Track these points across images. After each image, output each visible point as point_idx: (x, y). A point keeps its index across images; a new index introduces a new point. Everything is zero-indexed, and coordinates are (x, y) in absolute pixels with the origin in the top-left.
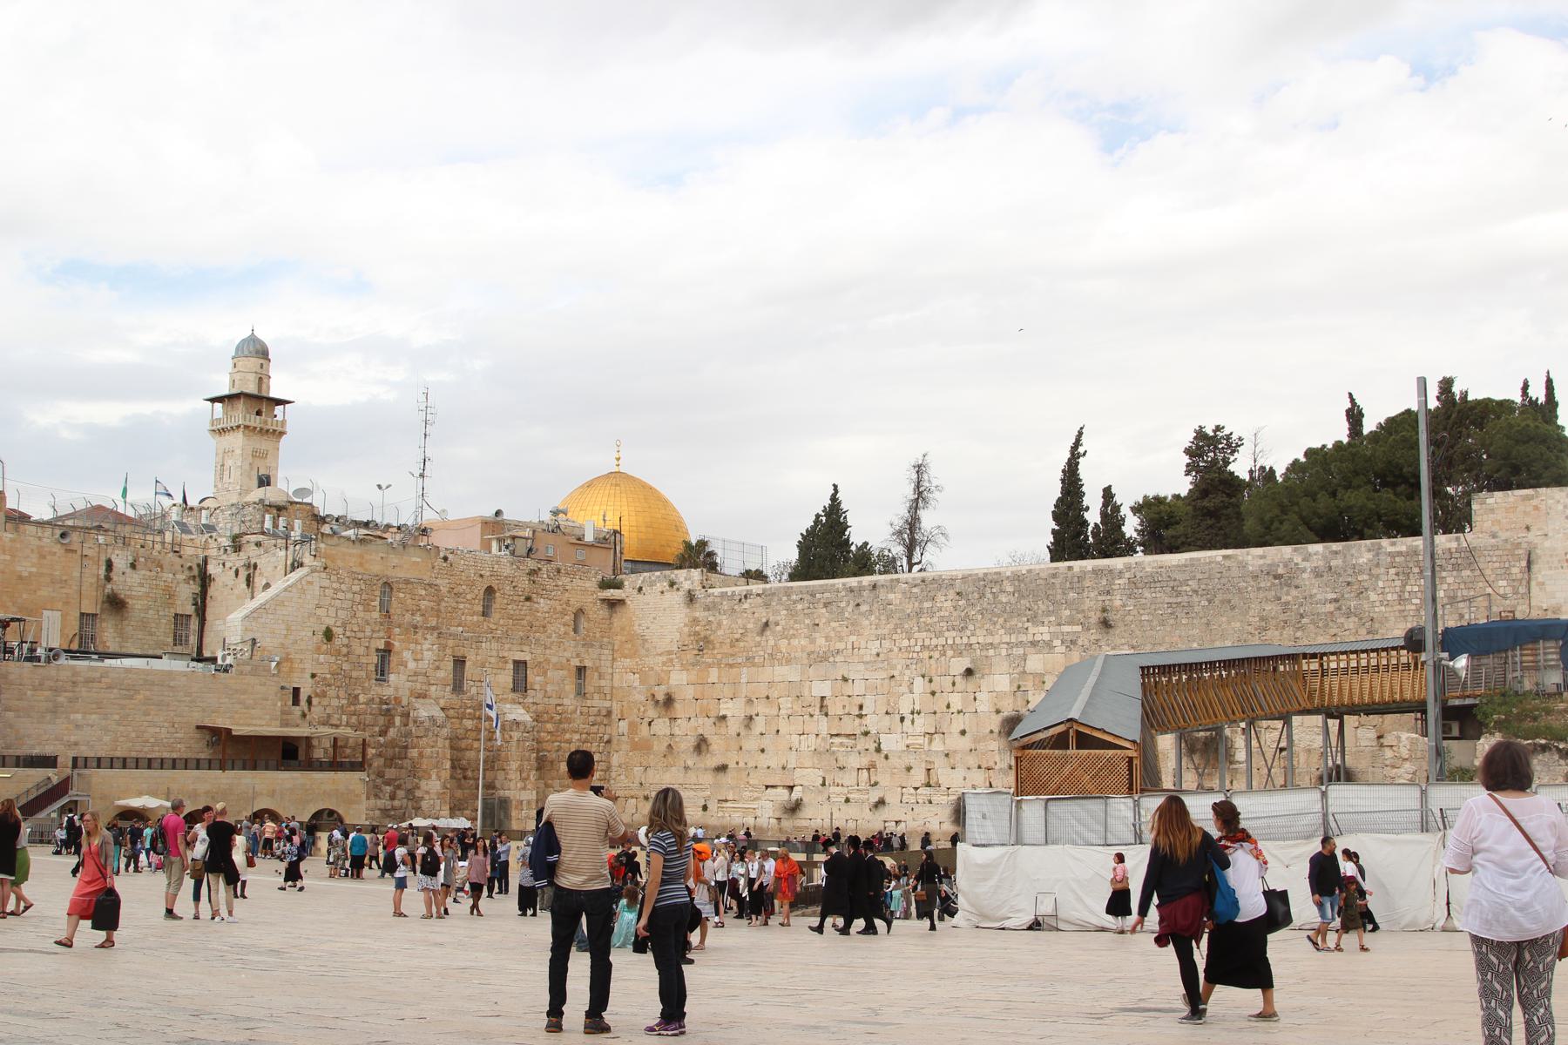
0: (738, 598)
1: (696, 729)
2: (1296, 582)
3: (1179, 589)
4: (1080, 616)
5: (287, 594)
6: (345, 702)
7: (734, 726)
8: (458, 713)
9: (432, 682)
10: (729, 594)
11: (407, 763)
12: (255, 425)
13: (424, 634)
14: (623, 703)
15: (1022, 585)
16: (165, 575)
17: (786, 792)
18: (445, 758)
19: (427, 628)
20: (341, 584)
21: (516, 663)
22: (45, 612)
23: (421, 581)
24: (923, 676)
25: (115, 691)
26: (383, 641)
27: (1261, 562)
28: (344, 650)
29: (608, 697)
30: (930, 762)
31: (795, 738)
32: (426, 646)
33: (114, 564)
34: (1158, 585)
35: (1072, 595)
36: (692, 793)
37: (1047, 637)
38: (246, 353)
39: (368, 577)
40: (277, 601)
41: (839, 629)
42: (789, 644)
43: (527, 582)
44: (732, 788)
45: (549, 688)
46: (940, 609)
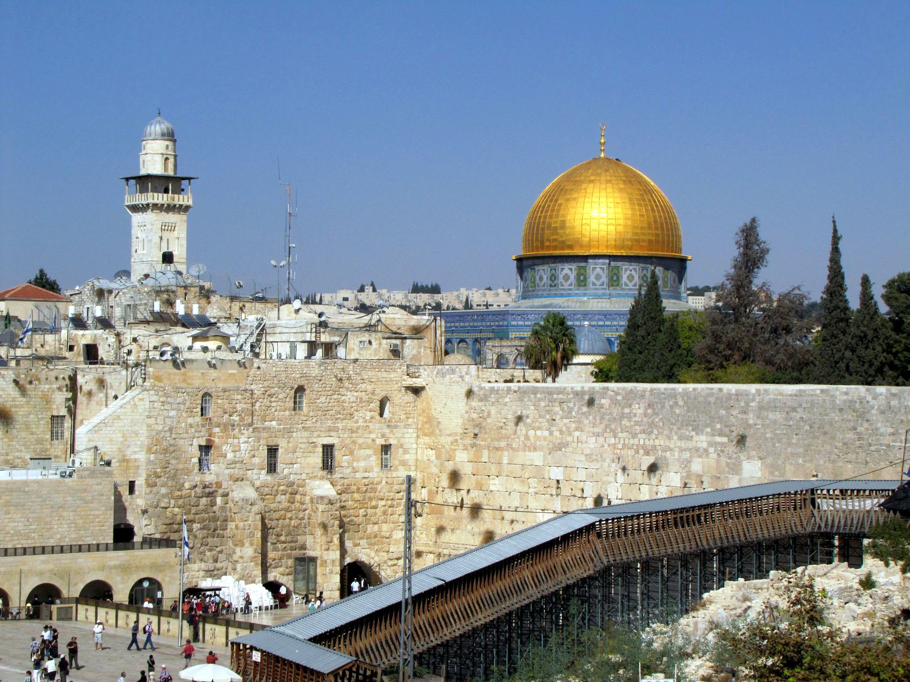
2: (868, 416)
5: (122, 410)
9: (248, 468)
10: (496, 388)
12: (163, 202)
13: (240, 431)
14: (425, 474)
16: (42, 386)
18: (256, 529)
19: (243, 425)
21: (324, 446)
24: (624, 469)
27: (845, 397)
28: (172, 449)
32: (243, 439)
35: (723, 412)
37: (705, 445)
39: (190, 390)
41: (568, 425)
43: (334, 379)
45: (355, 464)
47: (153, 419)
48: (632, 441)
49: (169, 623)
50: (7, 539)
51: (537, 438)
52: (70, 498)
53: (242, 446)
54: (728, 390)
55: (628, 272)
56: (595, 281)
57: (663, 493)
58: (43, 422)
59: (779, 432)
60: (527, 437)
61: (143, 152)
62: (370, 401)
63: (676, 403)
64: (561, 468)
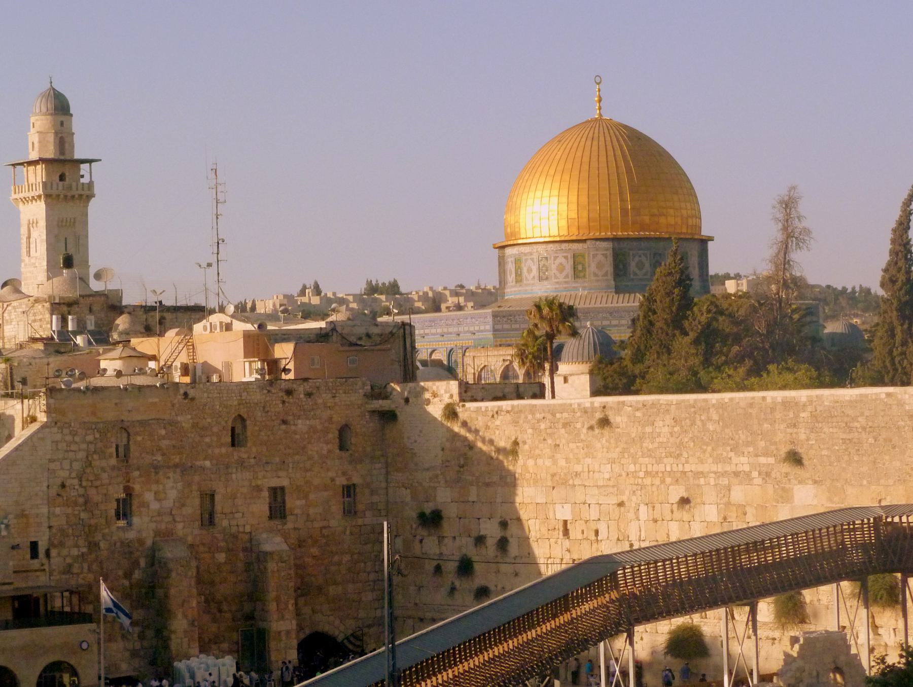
0: (490, 414)
1: (460, 548)
3: (851, 425)
4: (773, 447)
6: (85, 550)
10: (483, 409)
15: (726, 414)
19: (169, 467)
26: (121, 487)
28: (81, 500)
29: (383, 513)
34: (835, 420)
35: (766, 426)
37: (747, 468)
41: (576, 451)
43: (281, 405)
45: (312, 511)
54: (772, 398)
55: (637, 259)
57: (697, 531)
59: (837, 448)
61: (33, 131)
63: (710, 419)
64: (568, 507)
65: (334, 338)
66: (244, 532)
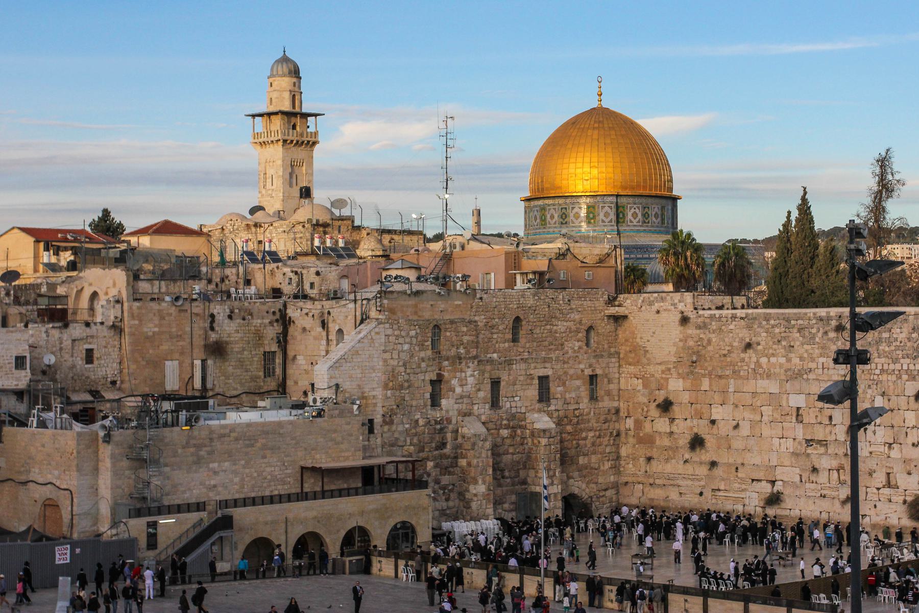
0: (725, 320)
1: (691, 428)
6: (407, 426)
7: (724, 428)
8: (496, 425)
9: (474, 402)
10: (717, 316)
11: (457, 470)
12: (292, 139)
13: (467, 363)
14: (630, 404)
16: (255, 321)
17: (769, 486)
20: (401, 331)
21: (540, 378)
22: (166, 362)
23: (463, 320)
25: (241, 442)
28: (406, 384)
30: (890, 467)
31: (776, 441)
32: (469, 373)
33: (216, 318)
36: (690, 483)
38: (280, 73)
39: (421, 322)
40: (355, 352)
41: (811, 351)
42: (769, 361)
43: (547, 309)
44: (723, 480)
45: (567, 396)
46: (896, 340)
47: (388, 354)
48: (892, 367)
49: (380, 562)
50: (265, 485)
51: (774, 365)
52: (322, 440)
53: (468, 379)
55: (633, 210)
56: (604, 219)
58: (255, 359)
60: (757, 362)
62: (578, 331)
65: (569, 256)
66: (520, 413)
